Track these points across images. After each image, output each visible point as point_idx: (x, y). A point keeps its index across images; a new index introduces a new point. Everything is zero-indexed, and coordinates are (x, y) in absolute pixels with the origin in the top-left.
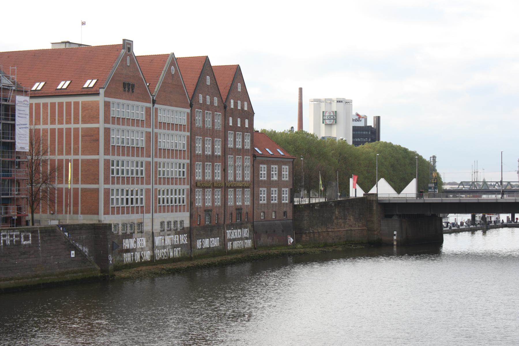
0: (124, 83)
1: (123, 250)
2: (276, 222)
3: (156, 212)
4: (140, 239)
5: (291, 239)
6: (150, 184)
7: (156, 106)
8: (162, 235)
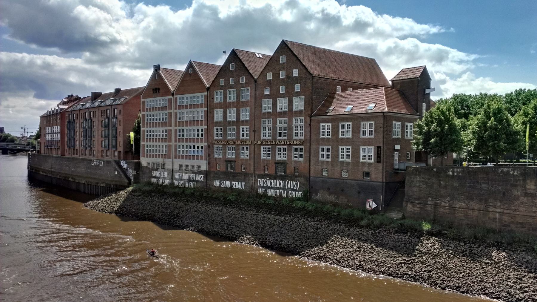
2: (348, 181)
3: (176, 158)
5: (374, 203)
6: (171, 142)
7: (175, 96)
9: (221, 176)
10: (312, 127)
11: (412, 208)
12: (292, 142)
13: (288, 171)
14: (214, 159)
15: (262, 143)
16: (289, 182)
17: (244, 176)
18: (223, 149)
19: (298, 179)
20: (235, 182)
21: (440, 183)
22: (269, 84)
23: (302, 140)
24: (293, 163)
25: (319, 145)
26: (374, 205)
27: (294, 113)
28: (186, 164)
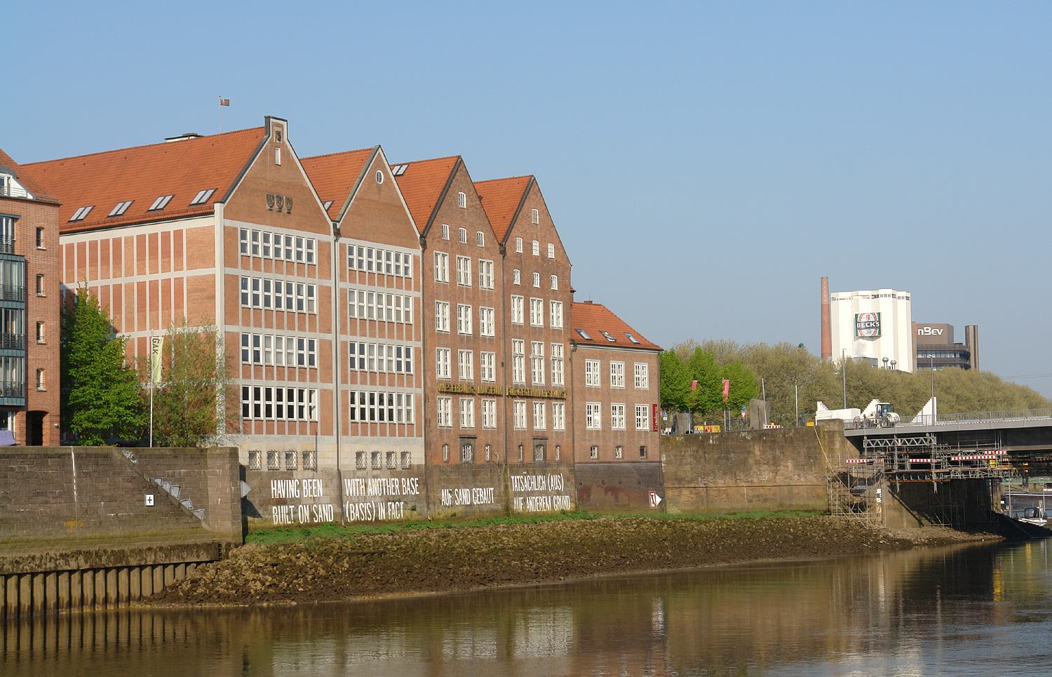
1: (270, 499)
2: (624, 465)
3: (345, 433)
7: (342, 240)
8: (361, 476)
9: (453, 476)
14: (438, 433)
25: (585, 400)
28: (374, 449)
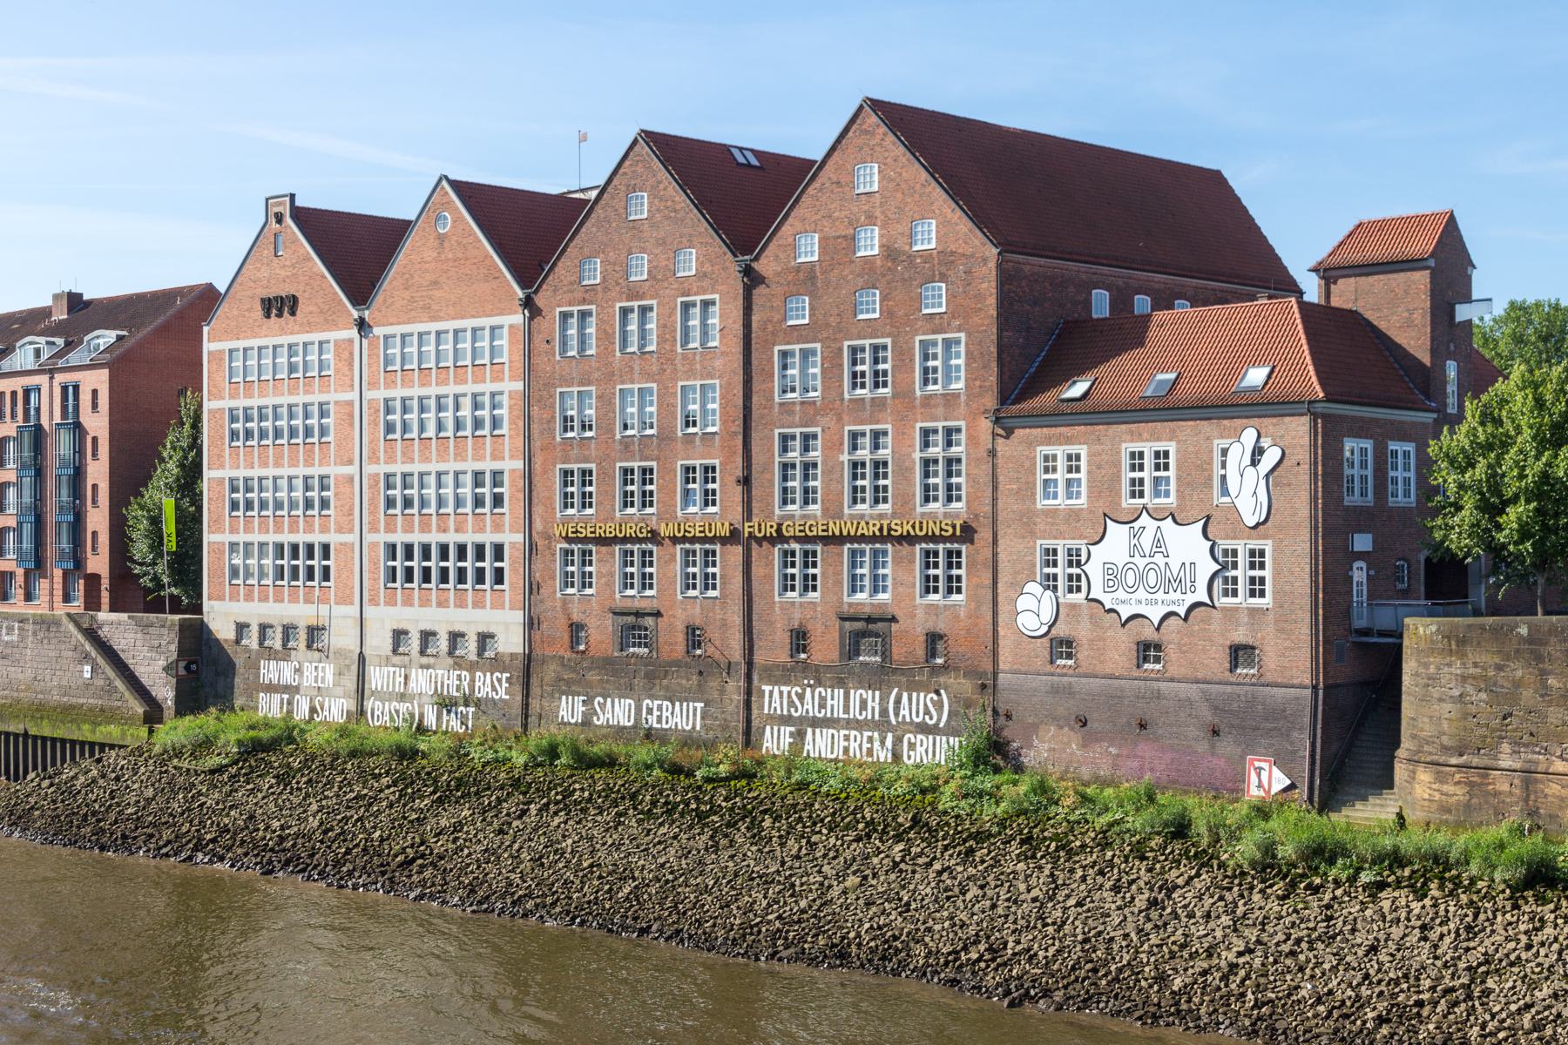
0: (263, 300)
2: (1163, 685)
3: (374, 602)
4: (314, 664)
5: (1276, 772)
6: (351, 531)
9: (593, 676)
10: (1000, 461)
11: (1434, 786)
12: (914, 527)
13: (898, 651)
14: (559, 604)
15: (779, 530)
16: (905, 695)
17: (701, 673)
18: (599, 561)
19: (942, 679)
20: (656, 703)
21: (1546, 687)
22: (807, 279)
23: (957, 516)
24: (920, 613)
25: (1033, 535)
26: (1280, 781)
27: (918, 402)
